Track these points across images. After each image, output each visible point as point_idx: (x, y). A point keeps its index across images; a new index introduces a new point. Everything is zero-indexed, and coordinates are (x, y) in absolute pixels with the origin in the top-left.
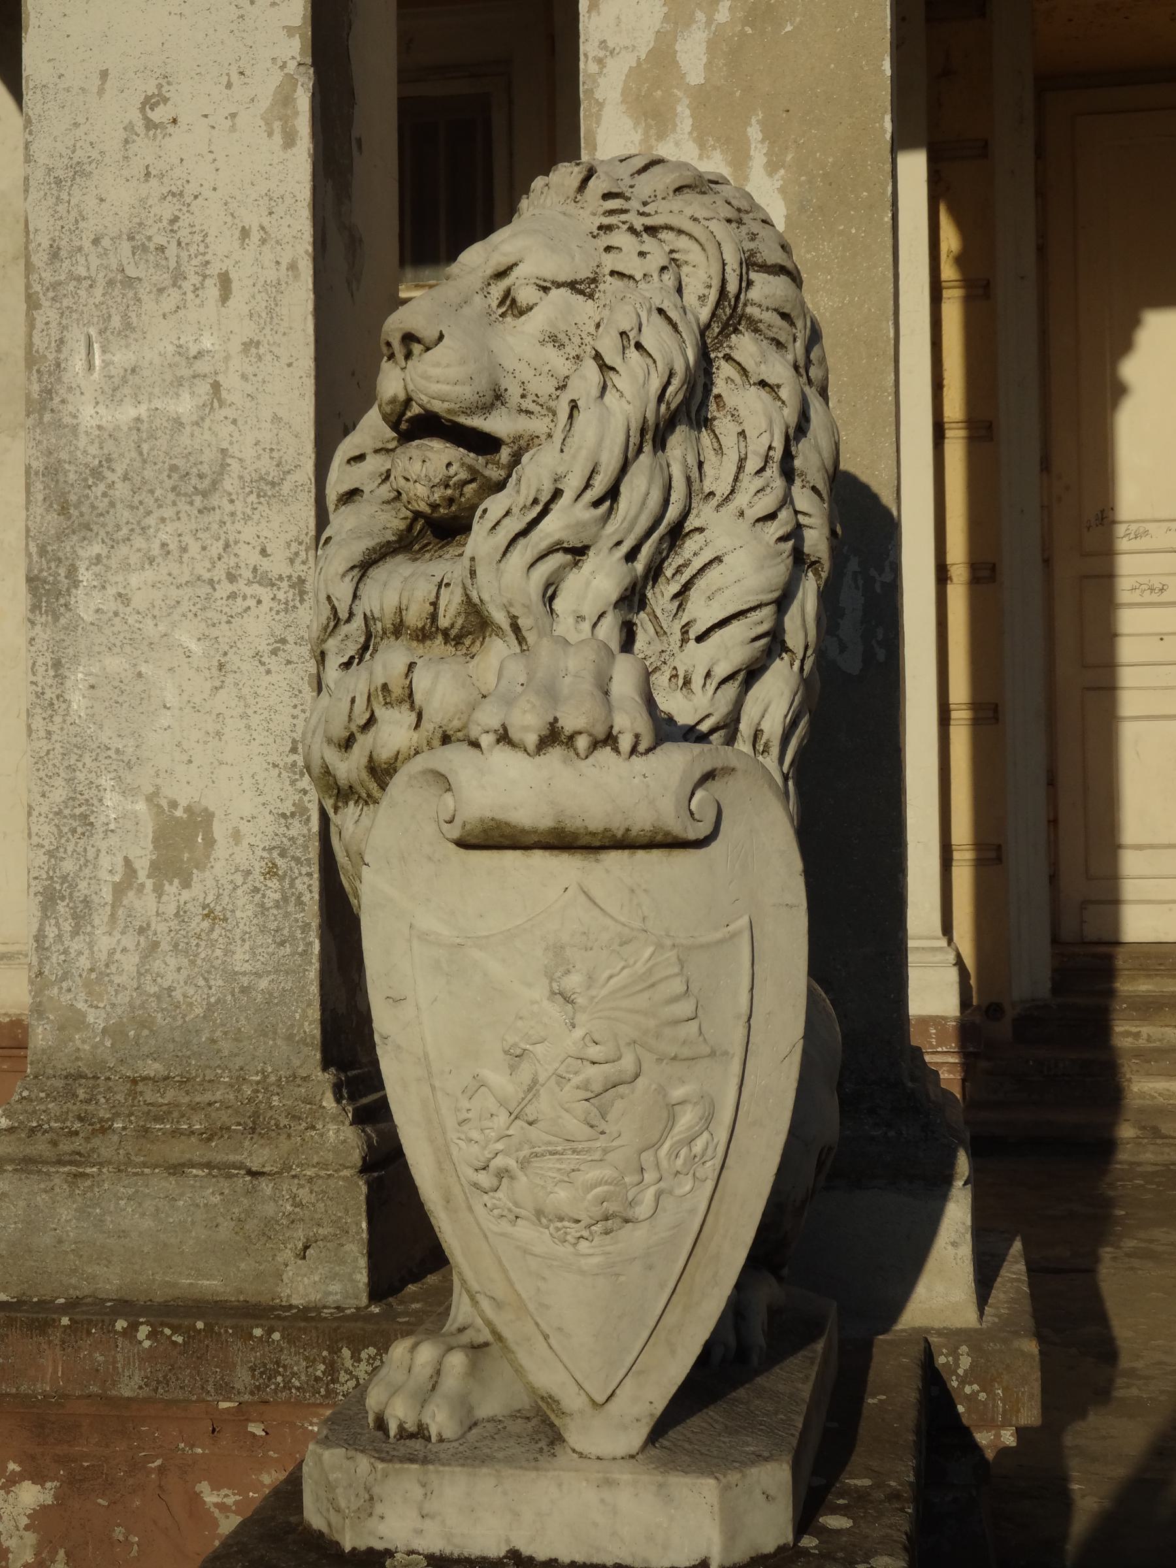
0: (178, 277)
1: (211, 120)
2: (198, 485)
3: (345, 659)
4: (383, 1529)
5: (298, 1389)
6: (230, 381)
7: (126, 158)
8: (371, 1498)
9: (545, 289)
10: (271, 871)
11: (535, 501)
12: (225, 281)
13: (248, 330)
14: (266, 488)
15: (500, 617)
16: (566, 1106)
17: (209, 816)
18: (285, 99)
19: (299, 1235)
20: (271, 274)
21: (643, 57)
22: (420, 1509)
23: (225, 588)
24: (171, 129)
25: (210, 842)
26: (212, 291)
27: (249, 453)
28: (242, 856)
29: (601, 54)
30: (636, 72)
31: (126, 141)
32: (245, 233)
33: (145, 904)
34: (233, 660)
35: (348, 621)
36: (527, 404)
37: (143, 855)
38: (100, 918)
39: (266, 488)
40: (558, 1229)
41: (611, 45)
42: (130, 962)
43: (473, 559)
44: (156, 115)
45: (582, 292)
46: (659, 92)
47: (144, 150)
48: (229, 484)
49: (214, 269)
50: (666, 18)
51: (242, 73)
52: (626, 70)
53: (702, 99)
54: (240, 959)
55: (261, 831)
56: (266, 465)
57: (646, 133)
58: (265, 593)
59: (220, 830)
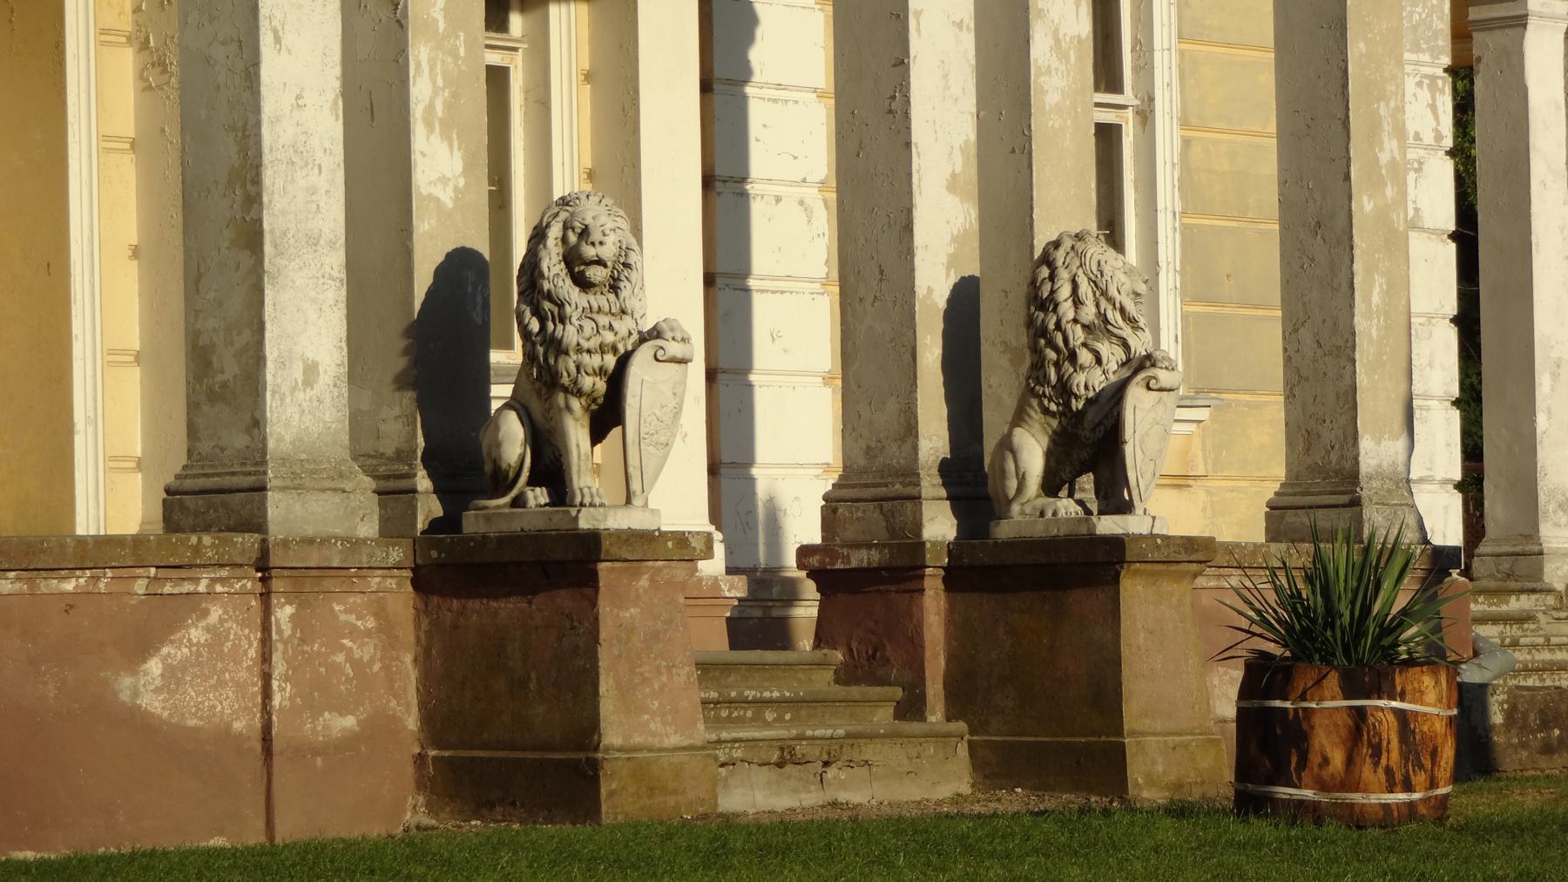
0: (307, 164)
2: (313, 241)
18: (335, 103)
19: (361, 513)
33: (300, 395)
37: (299, 375)
38: (288, 400)
42: (296, 417)
53: (442, 122)
59: (321, 370)
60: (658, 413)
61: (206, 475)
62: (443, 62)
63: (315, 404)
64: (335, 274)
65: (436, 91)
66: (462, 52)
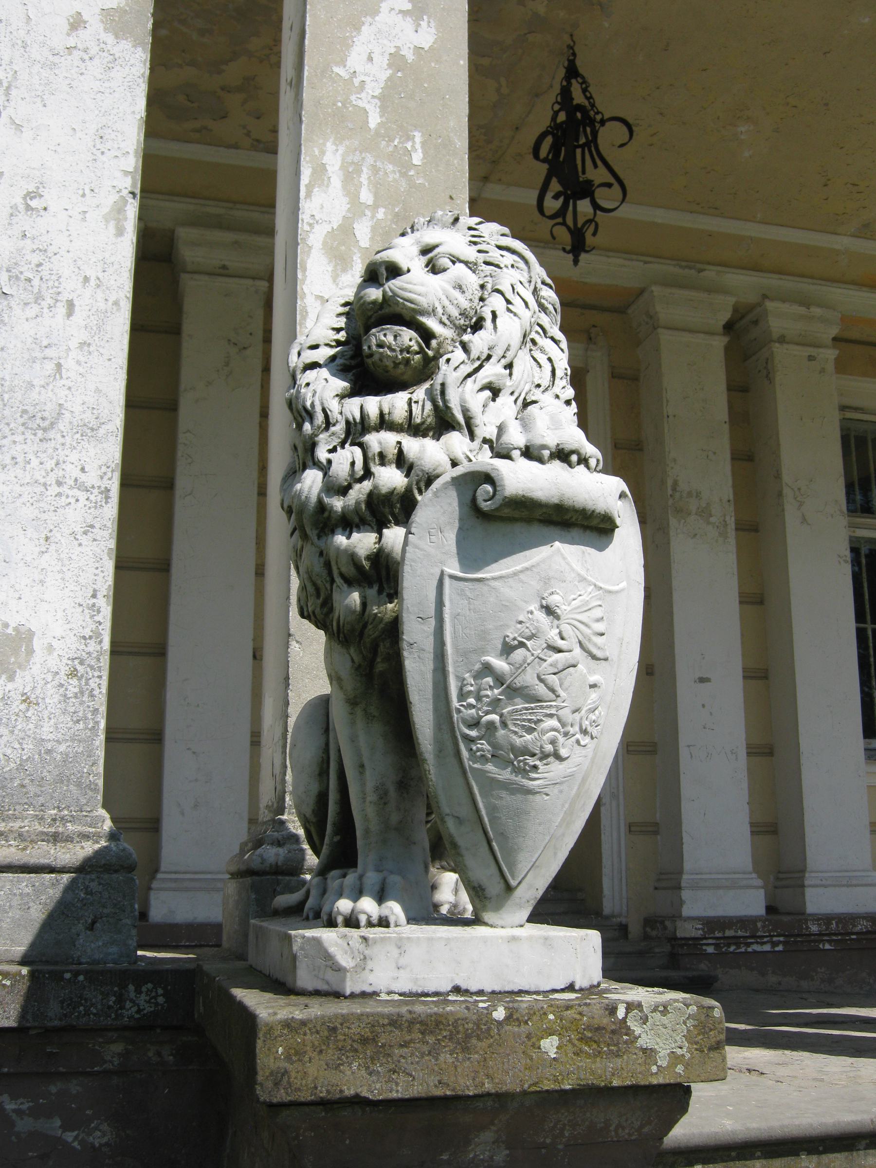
0: (38, 298)
1: (70, 213)
2: (42, 425)
3: (331, 447)
4: (371, 978)
5: (95, 1014)
6: (69, 364)
7: (10, 224)
8: (365, 958)
9: (454, 263)
10: (73, 673)
11: (478, 359)
12: (71, 306)
13: (84, 336)
14: (89, 431)
15: (460, 418)
16: (543, 677)
17: (31, 634)
18: (119, 209)
20: (102, 305)
21: (335, 228)
22: (397, 963)
23: (54, 490)
24: (42, 213)
25: (30, 652)
26: (61, 310)
27: (78, 409)
28: (53, 662)
29: (311, 222)
30: (331, 234)
31: (12, 215)
32: (86, 279)
34: (56, 535)
35: (334, 425)
36: (444, 319)
39: (89, 431)
40: (520, 761)
41: (317, 218)
43: (443, 385)
44: (34, 203)
45: (470, 268)
46: (343, 248)
47: (24, 222)
48: (61, 426)
49: (65, 297)
50: (349, 210)
51: (92, 190)
52: (325, 232)
54: (47, 731)
55: (70, 646)
56: (88, 417)
57: (335, 266)
58: (82, 496)
59: (37, 644)
60: (500, 664)
61: (55, 838)
62: (375, 170)
63: (17, 706)
64: (91, 478)
65: (356, 209)
66: (417, 158)
